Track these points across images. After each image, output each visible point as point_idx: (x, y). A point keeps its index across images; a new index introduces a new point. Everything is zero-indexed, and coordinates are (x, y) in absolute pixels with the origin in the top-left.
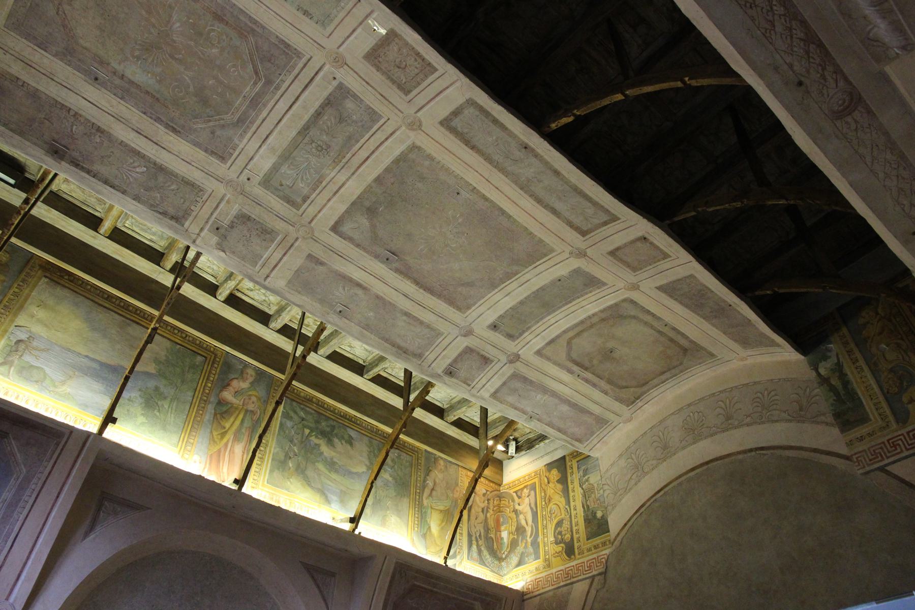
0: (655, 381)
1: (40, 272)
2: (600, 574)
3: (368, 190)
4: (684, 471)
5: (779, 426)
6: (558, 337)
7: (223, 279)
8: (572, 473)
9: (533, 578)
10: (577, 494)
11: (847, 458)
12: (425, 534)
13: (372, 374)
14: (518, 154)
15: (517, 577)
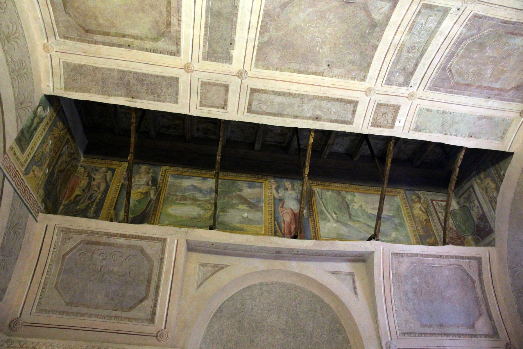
3: (379, 39)
5: (10, 90)
11: (5, 151)
14: (318, 113)
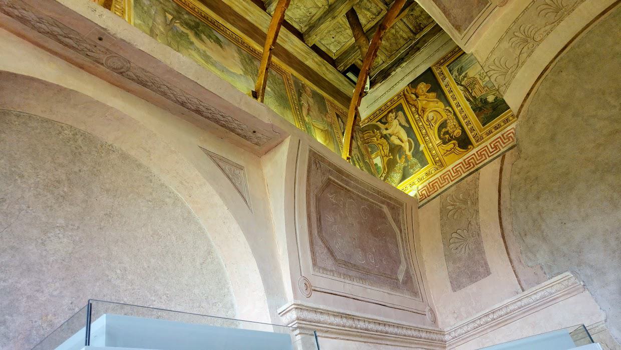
4: (592, 19)
8: (444, 78)
9: (426, 183)
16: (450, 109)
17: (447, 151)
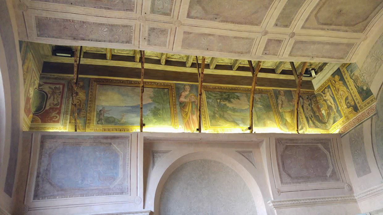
0: (373, 14)
1: (95, 83)
2: (375, 115)
6: (309, 17)
7: (160, 56)
9: (343, 126)
10: (350, 83)
12: (285, 124)
13: (236, 67)
15: (335, 128)
16: (349, 91)
17: (350, 112)
